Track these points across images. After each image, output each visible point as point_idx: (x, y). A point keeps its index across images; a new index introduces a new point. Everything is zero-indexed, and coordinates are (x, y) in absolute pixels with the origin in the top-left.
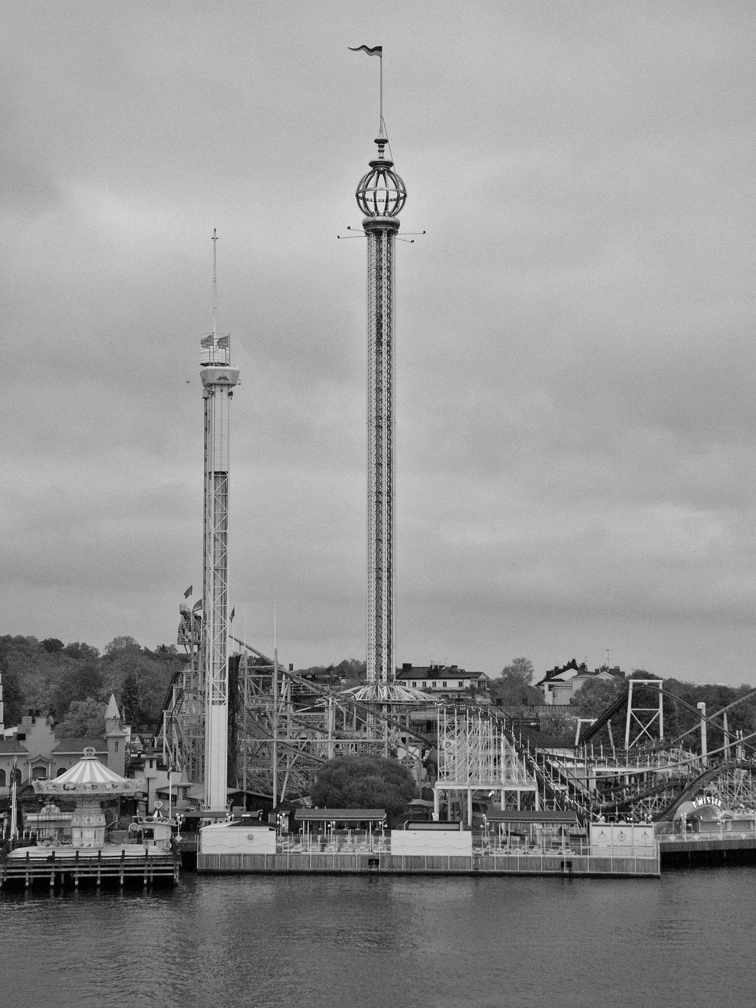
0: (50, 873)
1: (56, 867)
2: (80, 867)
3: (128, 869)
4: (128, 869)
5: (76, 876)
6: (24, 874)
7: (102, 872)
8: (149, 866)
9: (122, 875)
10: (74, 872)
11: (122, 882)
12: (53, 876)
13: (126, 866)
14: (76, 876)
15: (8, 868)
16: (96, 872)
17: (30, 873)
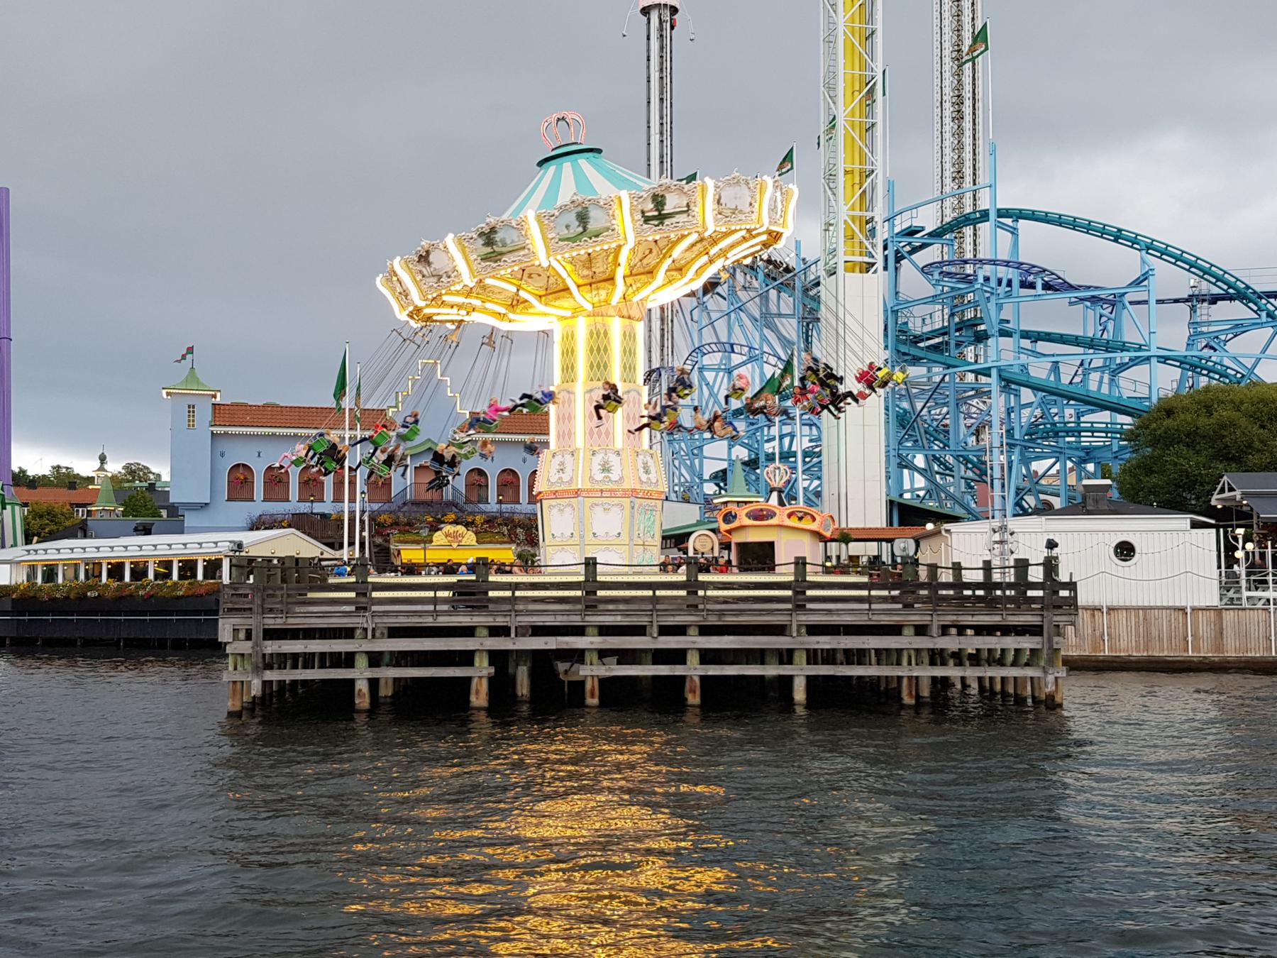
0: (466, 658)
1: (496, 631)
2: (605, 631)
3: (825, 642)
4: (825, 642)
5: (591, 671)
6: (347, 660)
7: (708, 657)
8: (921, 630)
9: (800, 672)
10: (577, 656)
11: (799, 694)
12: (481, 670)
13: (814, 630)
14: (591, 671)
15: (271, 634)
16: (678, 657)
17: (375, 659)
